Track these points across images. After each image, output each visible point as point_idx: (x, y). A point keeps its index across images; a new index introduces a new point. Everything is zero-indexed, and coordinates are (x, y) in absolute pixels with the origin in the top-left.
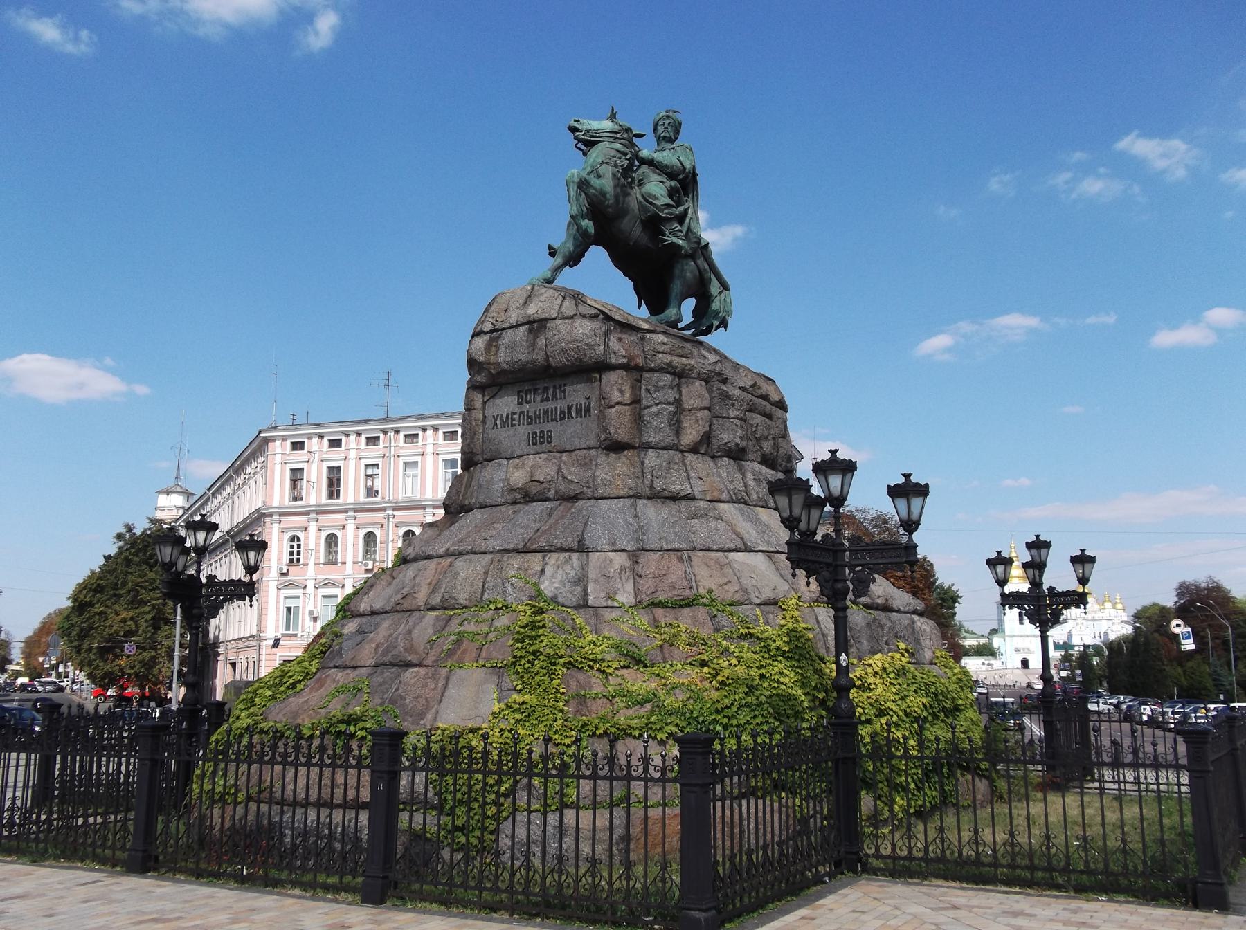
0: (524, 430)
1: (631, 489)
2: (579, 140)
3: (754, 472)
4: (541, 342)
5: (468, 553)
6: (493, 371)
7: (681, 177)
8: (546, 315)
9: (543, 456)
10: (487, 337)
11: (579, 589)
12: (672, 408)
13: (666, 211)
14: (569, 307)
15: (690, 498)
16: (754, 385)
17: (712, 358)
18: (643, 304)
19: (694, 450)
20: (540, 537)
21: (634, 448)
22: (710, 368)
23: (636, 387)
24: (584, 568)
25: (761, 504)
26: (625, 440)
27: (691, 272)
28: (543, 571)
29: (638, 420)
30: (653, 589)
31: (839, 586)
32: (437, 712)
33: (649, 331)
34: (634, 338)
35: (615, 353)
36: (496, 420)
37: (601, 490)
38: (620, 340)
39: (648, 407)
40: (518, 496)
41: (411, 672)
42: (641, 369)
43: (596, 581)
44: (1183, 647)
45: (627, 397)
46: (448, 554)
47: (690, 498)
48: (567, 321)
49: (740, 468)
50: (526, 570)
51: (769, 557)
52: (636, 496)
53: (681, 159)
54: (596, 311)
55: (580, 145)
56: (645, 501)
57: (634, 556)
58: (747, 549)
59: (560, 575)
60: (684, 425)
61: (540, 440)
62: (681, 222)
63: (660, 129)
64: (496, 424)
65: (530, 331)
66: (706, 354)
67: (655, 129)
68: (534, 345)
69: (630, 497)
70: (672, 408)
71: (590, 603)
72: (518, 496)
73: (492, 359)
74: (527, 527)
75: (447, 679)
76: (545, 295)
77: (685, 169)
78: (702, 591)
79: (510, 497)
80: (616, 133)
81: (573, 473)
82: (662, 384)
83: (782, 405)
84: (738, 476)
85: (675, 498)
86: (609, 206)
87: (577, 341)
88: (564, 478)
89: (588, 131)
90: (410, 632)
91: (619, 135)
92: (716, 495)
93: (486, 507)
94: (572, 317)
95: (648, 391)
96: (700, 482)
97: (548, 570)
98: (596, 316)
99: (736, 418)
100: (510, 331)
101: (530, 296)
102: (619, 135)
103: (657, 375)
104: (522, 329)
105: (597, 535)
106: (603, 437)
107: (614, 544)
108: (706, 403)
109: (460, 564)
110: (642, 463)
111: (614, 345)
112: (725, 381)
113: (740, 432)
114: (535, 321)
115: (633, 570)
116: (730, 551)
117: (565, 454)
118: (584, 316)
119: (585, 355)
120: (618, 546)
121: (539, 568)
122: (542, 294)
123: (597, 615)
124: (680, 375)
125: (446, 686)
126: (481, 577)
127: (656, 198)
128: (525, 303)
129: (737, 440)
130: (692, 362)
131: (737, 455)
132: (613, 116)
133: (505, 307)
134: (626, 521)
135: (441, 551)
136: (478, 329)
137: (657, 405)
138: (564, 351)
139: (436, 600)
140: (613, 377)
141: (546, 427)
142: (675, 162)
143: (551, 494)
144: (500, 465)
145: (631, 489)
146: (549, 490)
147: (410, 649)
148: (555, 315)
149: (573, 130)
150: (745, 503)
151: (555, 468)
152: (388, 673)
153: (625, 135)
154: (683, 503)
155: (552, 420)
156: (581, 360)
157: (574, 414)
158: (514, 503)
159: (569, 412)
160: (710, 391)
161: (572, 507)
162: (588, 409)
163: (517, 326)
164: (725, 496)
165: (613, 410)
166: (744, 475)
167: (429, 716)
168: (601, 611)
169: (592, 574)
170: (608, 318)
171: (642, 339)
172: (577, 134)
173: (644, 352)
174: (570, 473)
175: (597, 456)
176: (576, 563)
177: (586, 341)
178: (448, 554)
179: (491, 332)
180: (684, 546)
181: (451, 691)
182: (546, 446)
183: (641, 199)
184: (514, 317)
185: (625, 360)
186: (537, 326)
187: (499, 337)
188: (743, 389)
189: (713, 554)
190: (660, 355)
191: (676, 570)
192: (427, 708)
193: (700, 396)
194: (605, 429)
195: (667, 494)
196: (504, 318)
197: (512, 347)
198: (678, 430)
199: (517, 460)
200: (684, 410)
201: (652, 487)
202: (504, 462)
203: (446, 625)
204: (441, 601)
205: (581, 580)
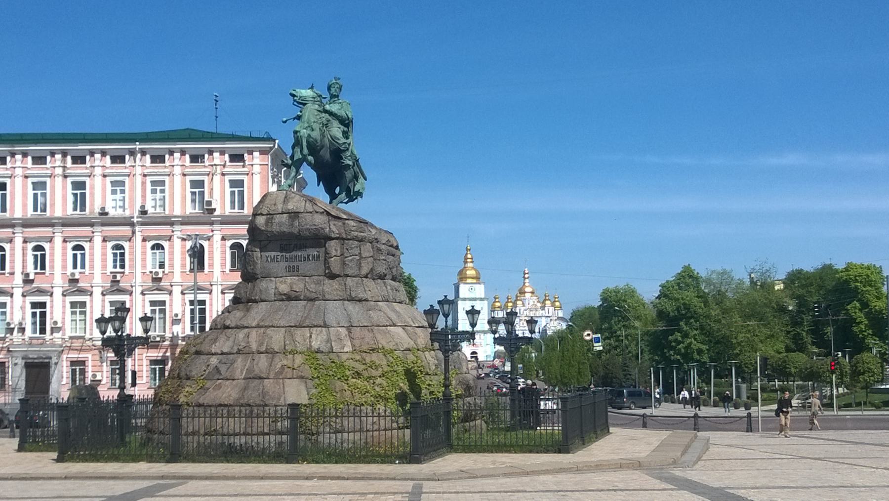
0: (283, 264)
1: (341, 296)
2: (295, 101)
3: (390, 285)
4: (296, 223)
5: (270, 327)
6: (269, 235)
7: (347, 122)
8: (297, 211)
9: (297, 278)
10: (265, 217)
11: (329, 345)
12: (358, 258)
13: (343, 146)
14: (309, 207)
15: (366, 300)
16: (388, 241)
17: (374, 231)
18: (321, 183)
19: (366, 277)
20: (305, 319)
21: (341, 277)
22: (373, 237)
23: (342, 248)
24: (329, 334)
25: (394, 301)
26: (338, 273)
27: (351, 174)
28: (311, 336)
29: (344, 264)
30: (359, 345)
31: (447, 348)
32: (285, 397)
33: (346, 219)
34: (340, 224)
35: (333, 232)
36: (267, 258)
37: (327, 297)
38: (334, 225)
39: (346, 257)
40: (284, 297)
41: (266, 380)
42: (343, 239)
43: (335, 341)
44: (595, 348)
45: (339, 253)
46: (258, 326)
47: (366, 300)
48: (309, 214)
49: (385, 283)
50: (303, 336)
51: (403, 329)
52: (344, 300)
53: (347, 113)
54: (323, 210)
55: (295, 103)
56: (347, 302)
57: (349, 328)
58: (394, 325)
59: (319, 338)
60: (362, 265)
61: (293, 271)
62: (348, 149)
63: (333, 90)
64: (267, 260)
65: (290, 217)
66: (371, 230)
67: (329, 89)
68: (292, 225)
69: (340, 300)
70: (358, 258)
71: (334, 351)
72: (284, 297)
73: (269, 229)
74: (297, 315)
75: (283, 384)
76: (296, 198)
77: (349, 118)
78: (380, 346)
79: (280, 297)
80: (314, 98)
81: (312, 287)
82: (353, 246)
83: (397, 248)
84: (384, 288)
85: (360, 301)
86: (318, 146)
87: (315, 225)
88: (308, 290)
89: (301, 97)
90: (257, 364)
91: (316, 99)
92: (377, 298)
93: (266, 301)
94: (311, 213)
95: (347, 249)
96: (370, 292)
97: (314, 336)
98: (323, 213)
99: (383, 260)
100: (278, 216)
101: (286, 197)
102: (316, 99)
103: (351, 241)
104: (285, 215)
105: (331, 319)
106: (327, 271)
107: (339, 324)
108: (372, 254)
109: (269, 331)
110: (345, 284)
111: (334, 228)
112: (377, 242)
113: (385, 267)
114: (292, 213)
115: (349, 336)
116: (387, 326)
117: (307, 278)
118: (317, 212)
119: (319, 232)
120: (341, 325)
121: (309, 335)
122: (293, 198)
123: (338, 356)
124: (361, 240)
125: (284, 387)
126: (283, 339)
127: (339, 139)
128: (284, 201)
129: (384, 271)
130: (366, 235)
131: (382, 277)
132: (312, 88)
133: (273, 202)
134: (342, 313)
135: (254, 324)
136: (259, 212)
137: (351, 256)
138: (308, 229)
139: (263, 349)
140: (333, 243)
141: (296, 264)
142: (344, 114)
143: (302, 297)
144: (271, 280)
145: (341, 296)
146: (301, 296)
147: (261, 372)
148: (302, 211)
149: (294, 96)
150: (388, 301)
151: (303, 285)
152: (257, 382)
153: (319, 99)
154: (364, 302)
155: (299, 261)
156: (317, 235)
157: (311, 259)
158: (282, 300)
159: (308, 257)
160: (373, 248)
161: (314, 304)
162: (318, 257)
163: (282, 213)
164: (380, 299)
165: (332, 259)
166: (386, 288)
167: (282, 399)
168: (340, 354)
169: (333, 338)
170: (328, 214)
171: (344, 224)
172: (295, 98)
173: (345, 230)
174: (311, 288)
175: (324, 280)
176: (324, 332)
177: (320, 226)
178: (258, 326)
179: (267, 215)
180: (369, 324)
181: (286, 389)
182: (296, 273)
183: (329, 137)
184: (280, 207)
185: (338, 236)
186: (294, 215)
187: (272, 218)
188: (383, 244)
189: (381, 328)
190: (353, 232)
191: (368, 336)
192: (281, 396)
193: (369, 251)
194: (329, 268)
195: (357, 299)
196: (274, 208)
197: (280, 224)
198: (360, 267)
199: (281, 279)
200: (362, 258)
201: (350, 296)
202: (273, 279)
203: (272, 361)
204: (266, 350)
205: (329, 340)
